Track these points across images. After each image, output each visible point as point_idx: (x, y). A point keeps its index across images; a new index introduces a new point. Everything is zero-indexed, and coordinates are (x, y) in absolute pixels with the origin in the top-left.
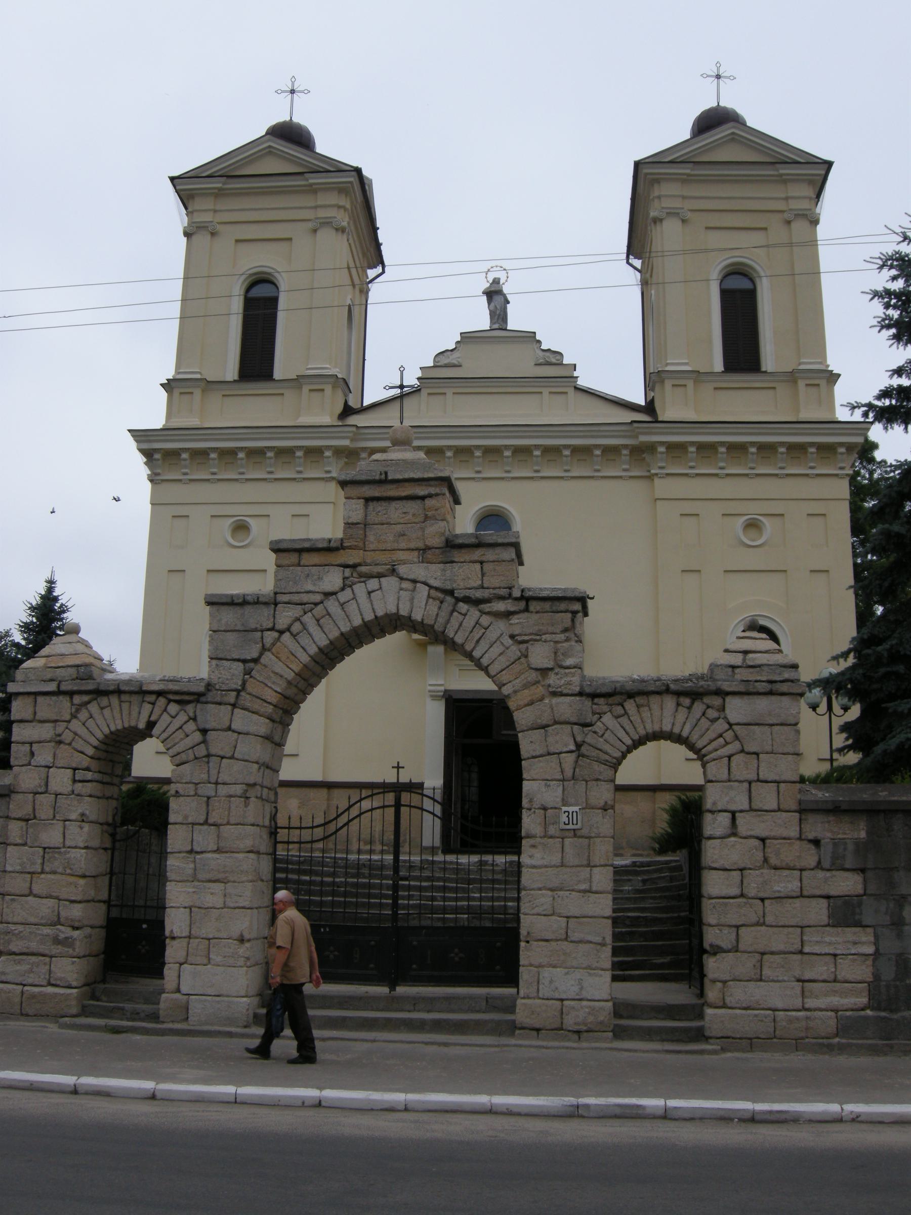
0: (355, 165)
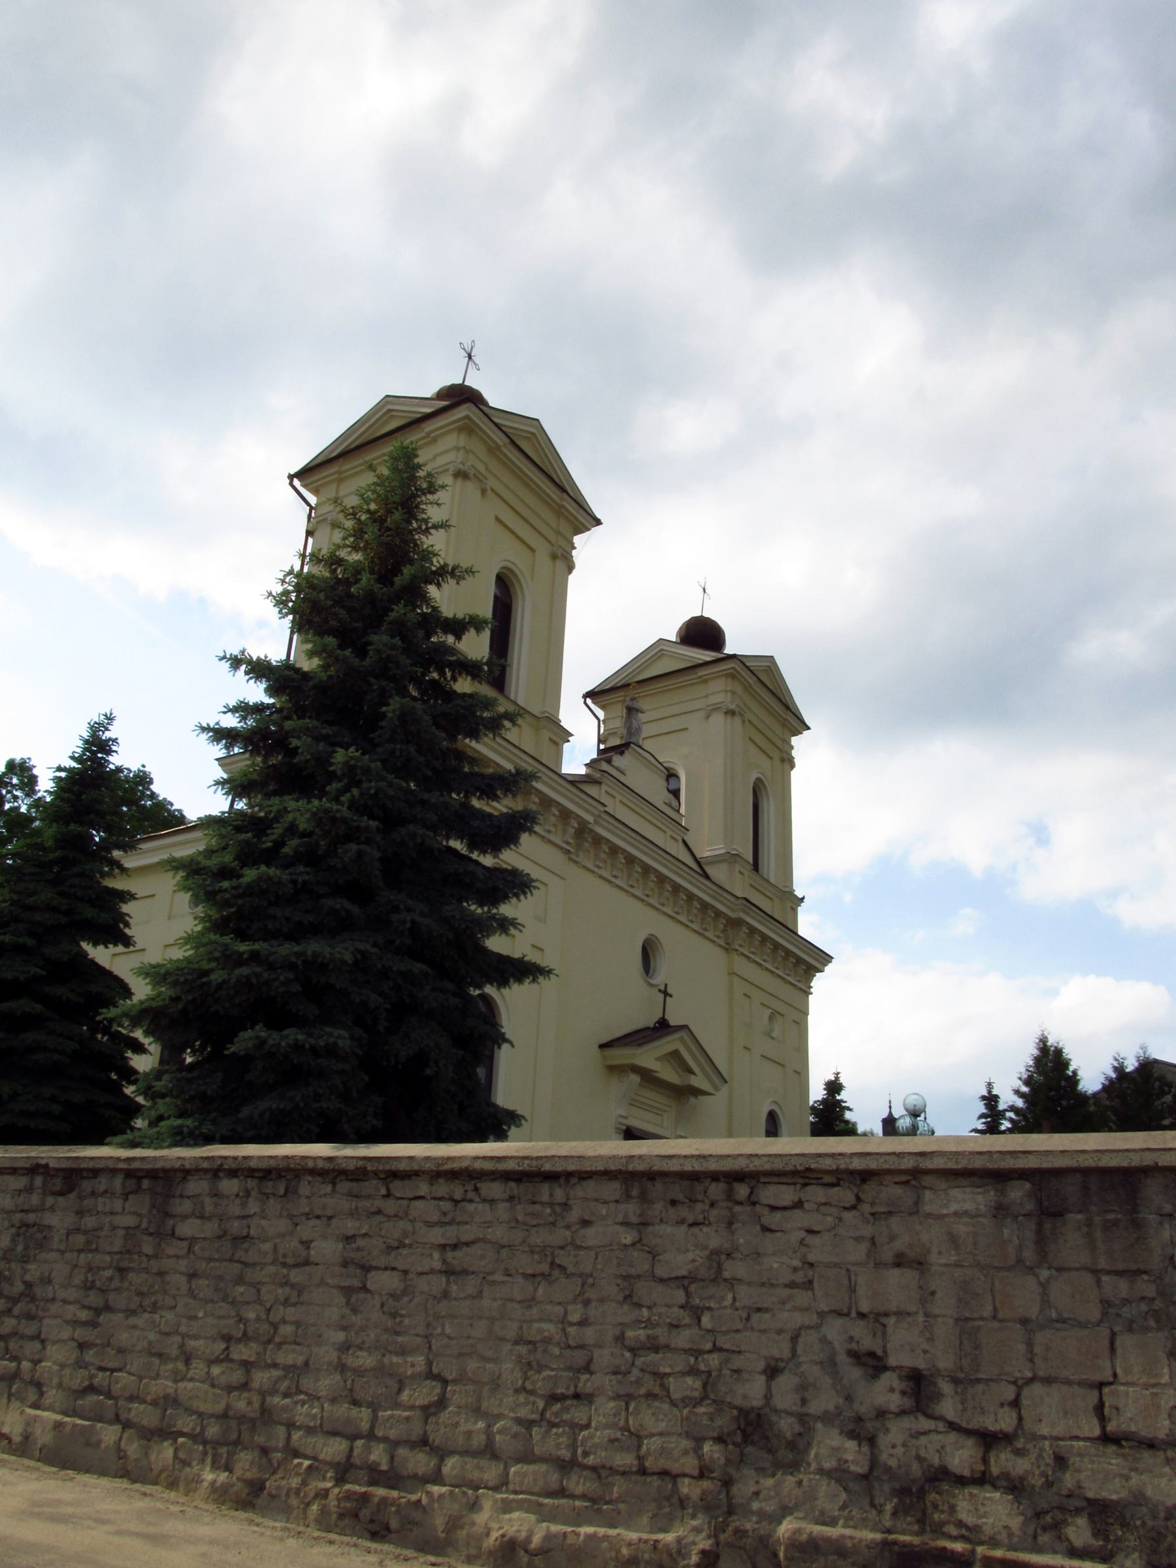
0: (598, 516)
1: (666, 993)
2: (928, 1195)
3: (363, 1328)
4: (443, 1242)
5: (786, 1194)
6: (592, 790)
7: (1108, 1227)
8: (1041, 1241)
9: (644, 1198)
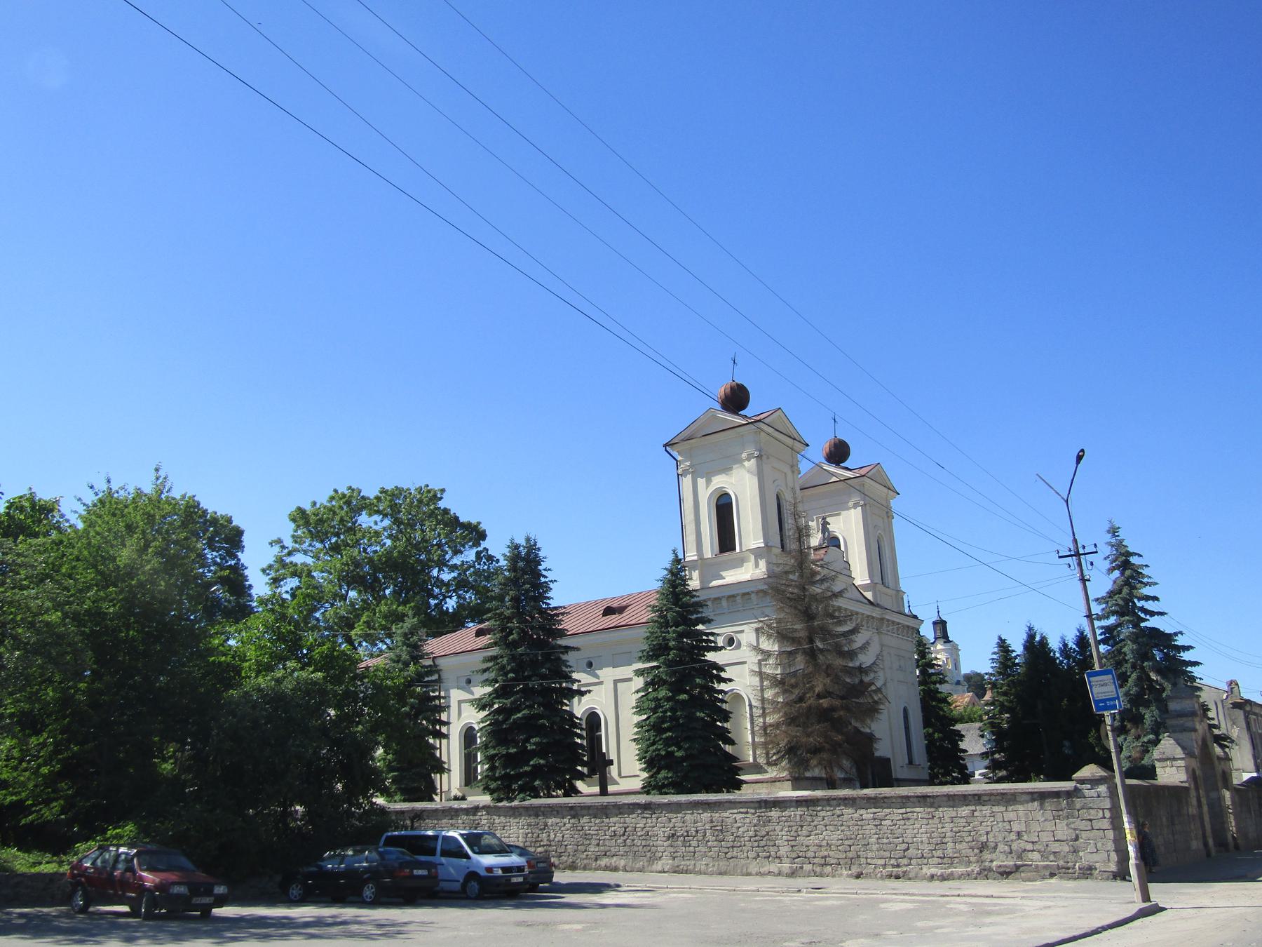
9: (953, 800)
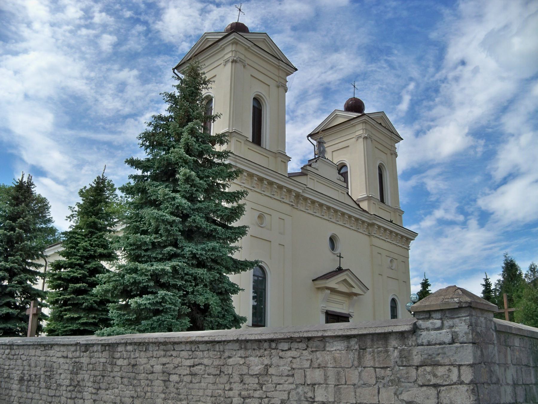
1: (340, 257)
2: (327, 344)
3: (170, 393)
4: (189, 365)
5: (285, 346)
6: (302, 179)
7: (379, 352)
8: (360, 358)
